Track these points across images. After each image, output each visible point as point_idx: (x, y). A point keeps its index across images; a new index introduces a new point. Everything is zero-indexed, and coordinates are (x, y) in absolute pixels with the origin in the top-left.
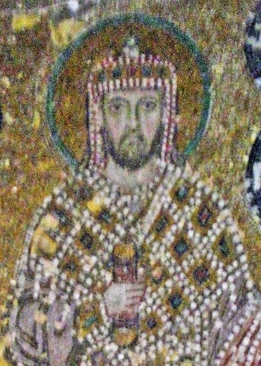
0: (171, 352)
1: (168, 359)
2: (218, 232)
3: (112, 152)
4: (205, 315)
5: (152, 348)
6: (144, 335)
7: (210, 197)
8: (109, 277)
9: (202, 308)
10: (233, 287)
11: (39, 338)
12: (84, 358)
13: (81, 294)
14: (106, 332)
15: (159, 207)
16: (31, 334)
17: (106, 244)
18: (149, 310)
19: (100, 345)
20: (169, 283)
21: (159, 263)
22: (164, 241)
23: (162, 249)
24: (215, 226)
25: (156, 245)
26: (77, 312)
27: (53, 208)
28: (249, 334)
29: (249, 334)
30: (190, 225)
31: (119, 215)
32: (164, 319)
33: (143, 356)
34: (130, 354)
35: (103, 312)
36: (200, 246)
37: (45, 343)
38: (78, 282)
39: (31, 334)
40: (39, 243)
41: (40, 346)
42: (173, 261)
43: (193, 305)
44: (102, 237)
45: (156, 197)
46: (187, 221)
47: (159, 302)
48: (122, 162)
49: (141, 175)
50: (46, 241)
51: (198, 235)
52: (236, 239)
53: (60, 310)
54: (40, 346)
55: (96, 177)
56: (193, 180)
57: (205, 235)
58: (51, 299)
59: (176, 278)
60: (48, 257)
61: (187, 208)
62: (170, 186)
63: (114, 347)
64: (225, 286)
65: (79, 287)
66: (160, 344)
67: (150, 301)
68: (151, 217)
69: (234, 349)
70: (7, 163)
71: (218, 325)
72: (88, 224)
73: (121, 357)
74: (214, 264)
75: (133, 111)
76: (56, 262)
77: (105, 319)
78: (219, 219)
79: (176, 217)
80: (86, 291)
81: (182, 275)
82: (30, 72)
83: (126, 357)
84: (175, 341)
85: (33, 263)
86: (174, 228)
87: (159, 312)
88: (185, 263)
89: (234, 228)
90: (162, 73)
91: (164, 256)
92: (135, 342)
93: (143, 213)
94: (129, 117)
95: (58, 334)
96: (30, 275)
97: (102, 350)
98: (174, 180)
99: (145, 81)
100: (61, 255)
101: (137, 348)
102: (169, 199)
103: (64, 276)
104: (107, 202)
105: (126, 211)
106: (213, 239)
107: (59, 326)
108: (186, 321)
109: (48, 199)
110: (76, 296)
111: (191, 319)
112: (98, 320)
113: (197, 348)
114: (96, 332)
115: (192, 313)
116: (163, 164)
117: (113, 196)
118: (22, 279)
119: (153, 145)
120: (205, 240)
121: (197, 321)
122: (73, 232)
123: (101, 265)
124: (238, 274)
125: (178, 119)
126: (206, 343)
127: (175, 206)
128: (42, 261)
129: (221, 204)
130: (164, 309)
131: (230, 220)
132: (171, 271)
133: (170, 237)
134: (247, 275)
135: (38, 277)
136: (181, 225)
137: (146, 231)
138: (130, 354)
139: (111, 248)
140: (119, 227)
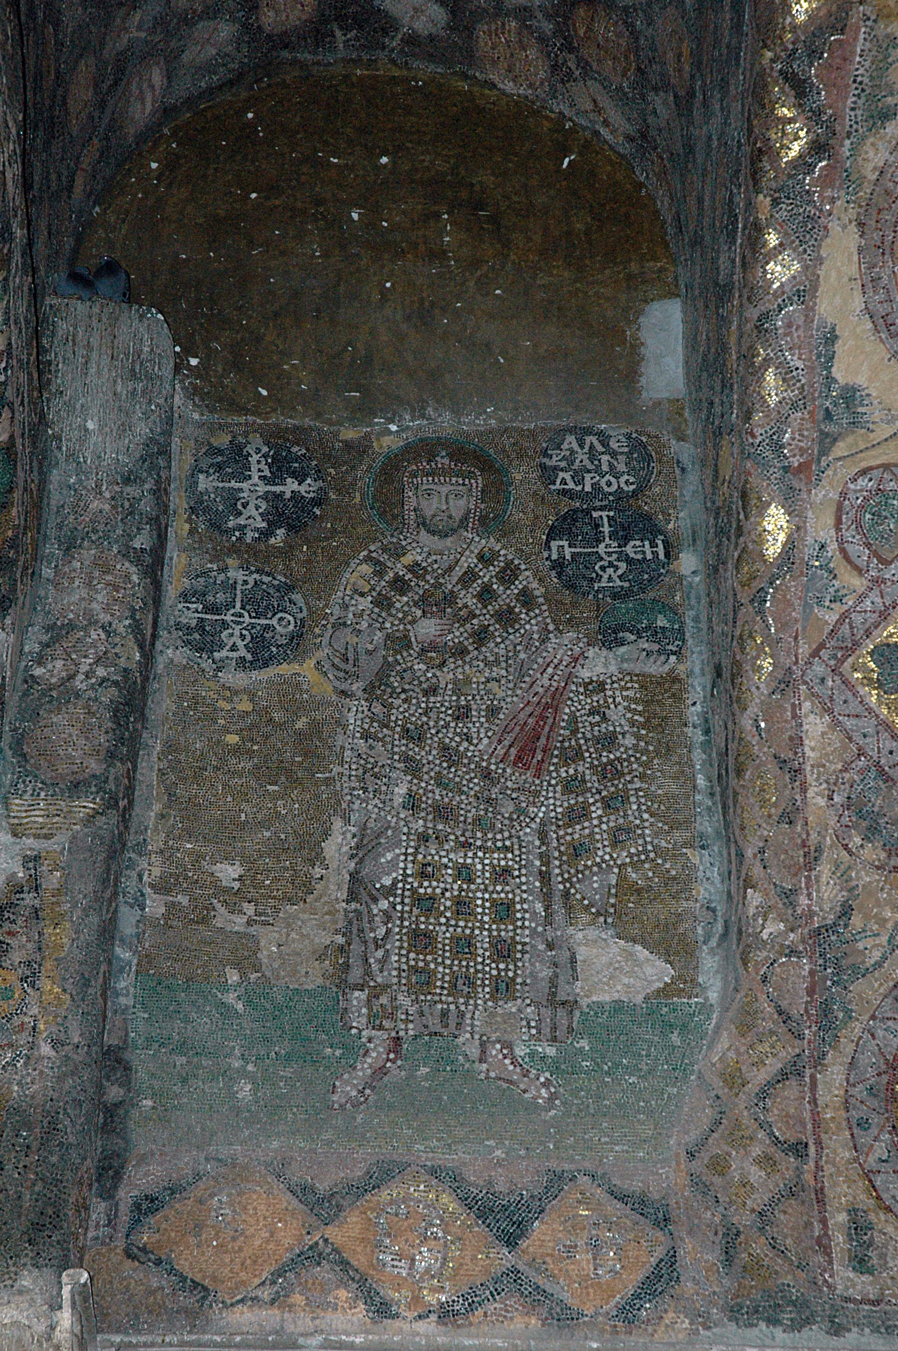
0: (478, 674)
1: (475, 680)
2: (520, 587)
3: (424, 524)
4: (511, 648)
5: (460, 670)
6: (452, 660)
7: (512, 561)
8: (419, 613)
9: (508, 642)
10: (535, 628)
11: (350, 655)
12: (394, 674)
13: (392, 624)
14: (416, 655)
15: (466, 565)
16: (343, 651)
17: (417, 589)
18: (456, 641)
19: (409, 664)
20: (475, 621)
21: (466, 606)
22: (471, 590)
23: (469, 595)
24: (517, 582)
25: (463, 592)
26: (388, 636)
27: (368, 559)
28: (552, 665)
29: (552, 665)
30: (494, 580)
31: (429, 569)
32: (471, 648)
33: (451, 676)
34: (438, 673)
35: (413, 639)
36: (504, 596)
37: (356, 660)
38: (390, 615)
39: (343, 651)
40: (354, 584)
41: (351, 662)
42: (479, 606)
43: (499, 640)
44: (413, 584)
45: (463, 558)
46: (492, 577)
47: (466, 635)
48: (433, 533)
49: (449, 541)
50: (361, 582)
51: (501, 588)
52: (537, 593)
53: (371, 634)
54: (351, 662)
55: (409, 540)
56: (497, 548)
57: (509, 588)
58: (365, 625)
59: (481, 618)
60: (362, 595)
61: (491, 568)
62: (476, 551)
63: (423, 667)
64: (528, 627)
65: (391, 619)
66: (467, 667)
67: (457, 634)
68: (458, 572)
69: (539, 676)
70: (329, 525)
71: (522, 656)
72: (401, 573)
73: (430, 675)
74: (517, 610)
75: (444, 499)
76: (370, 599)
77: (415, 644)
78: (520, 578)
79: (481, 574)
80: (396, 622)
81: (488, 616)
82: (353, 468)
83: (434, 675)
84: (482, 665)
85: (347, 598)
86: (479, 581)
87: (466, 643)
88: (490, 607)
89: (535, 585)
90: (470, 475)
91: (471, 601)
92: (443, 664)
93: (450, 569)
94: (440, 502)
95: (369, 653)
96: (345, 607)
97: (411, 668)
98: (480, 547)
99: (454, 480)
100: (374, 594)
101: (445, 670)
102: (475, 561)
103: (376, 610)
104: (419, 558)
105: (436, 566)
106: (516, 591)
107: (370, 647)
108: (492, 651)
109: (365, 553)
110: (388, 625)
111: (496, 650)
112: (409, 646)
113: (504, 673)
114: (405, 654)
115: (497, 644)
116: (470, 536)
117: (424, 555)
118: (337, 611)
119: (461, 521)
120: (508, 592)
121: (502, 652)
122: (387, 578)
123: (411, 604)
124: (540, 619)
125: (483, 506)
126: (511, 670)
127: (480, 566)
128: (356, 597)
129: (523, 567)
130: (471, 640)
131: (531, 579)
132: (478, 612)
133: (476, 587)
134: (549, 620)
135: (351, 609)
136: (485, 580)
137: (454, 582)
138: (438, 673)
139: (421, 592)
140: (428, 577)
